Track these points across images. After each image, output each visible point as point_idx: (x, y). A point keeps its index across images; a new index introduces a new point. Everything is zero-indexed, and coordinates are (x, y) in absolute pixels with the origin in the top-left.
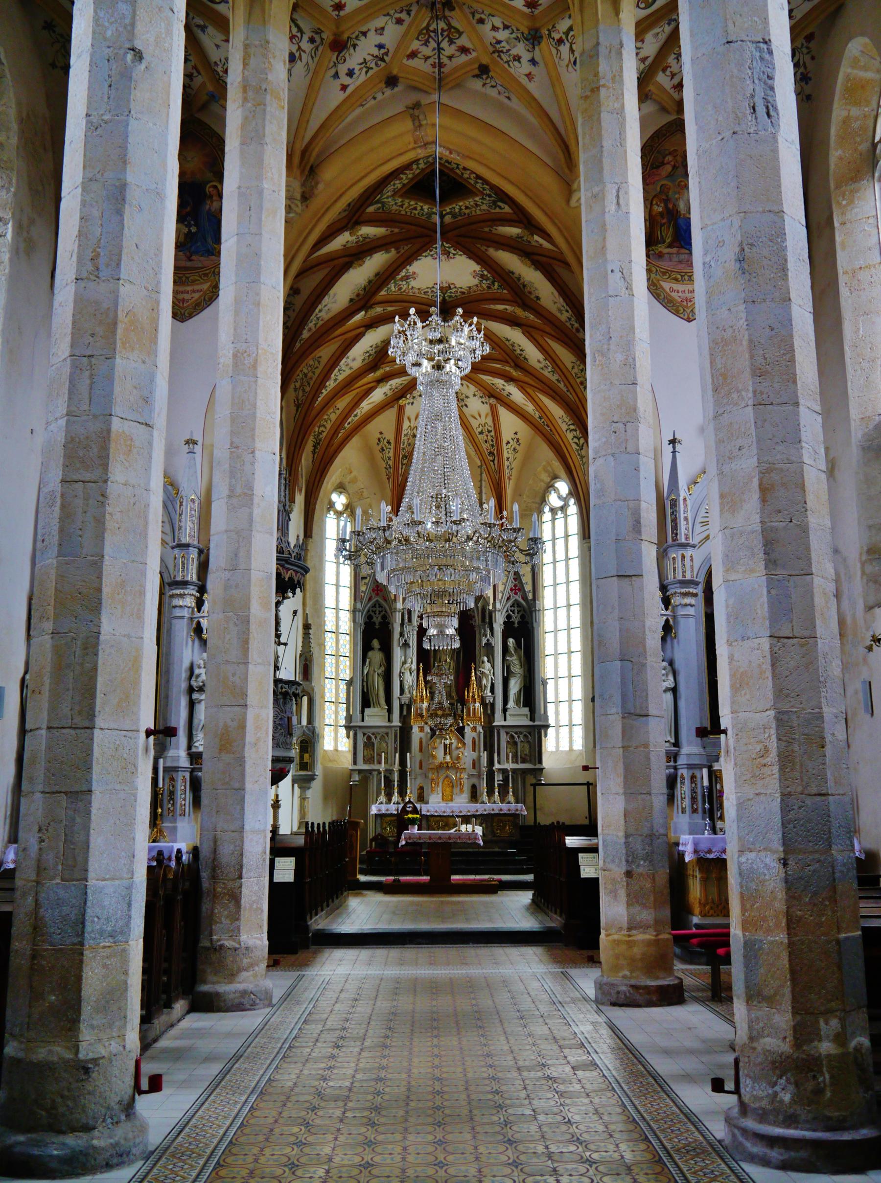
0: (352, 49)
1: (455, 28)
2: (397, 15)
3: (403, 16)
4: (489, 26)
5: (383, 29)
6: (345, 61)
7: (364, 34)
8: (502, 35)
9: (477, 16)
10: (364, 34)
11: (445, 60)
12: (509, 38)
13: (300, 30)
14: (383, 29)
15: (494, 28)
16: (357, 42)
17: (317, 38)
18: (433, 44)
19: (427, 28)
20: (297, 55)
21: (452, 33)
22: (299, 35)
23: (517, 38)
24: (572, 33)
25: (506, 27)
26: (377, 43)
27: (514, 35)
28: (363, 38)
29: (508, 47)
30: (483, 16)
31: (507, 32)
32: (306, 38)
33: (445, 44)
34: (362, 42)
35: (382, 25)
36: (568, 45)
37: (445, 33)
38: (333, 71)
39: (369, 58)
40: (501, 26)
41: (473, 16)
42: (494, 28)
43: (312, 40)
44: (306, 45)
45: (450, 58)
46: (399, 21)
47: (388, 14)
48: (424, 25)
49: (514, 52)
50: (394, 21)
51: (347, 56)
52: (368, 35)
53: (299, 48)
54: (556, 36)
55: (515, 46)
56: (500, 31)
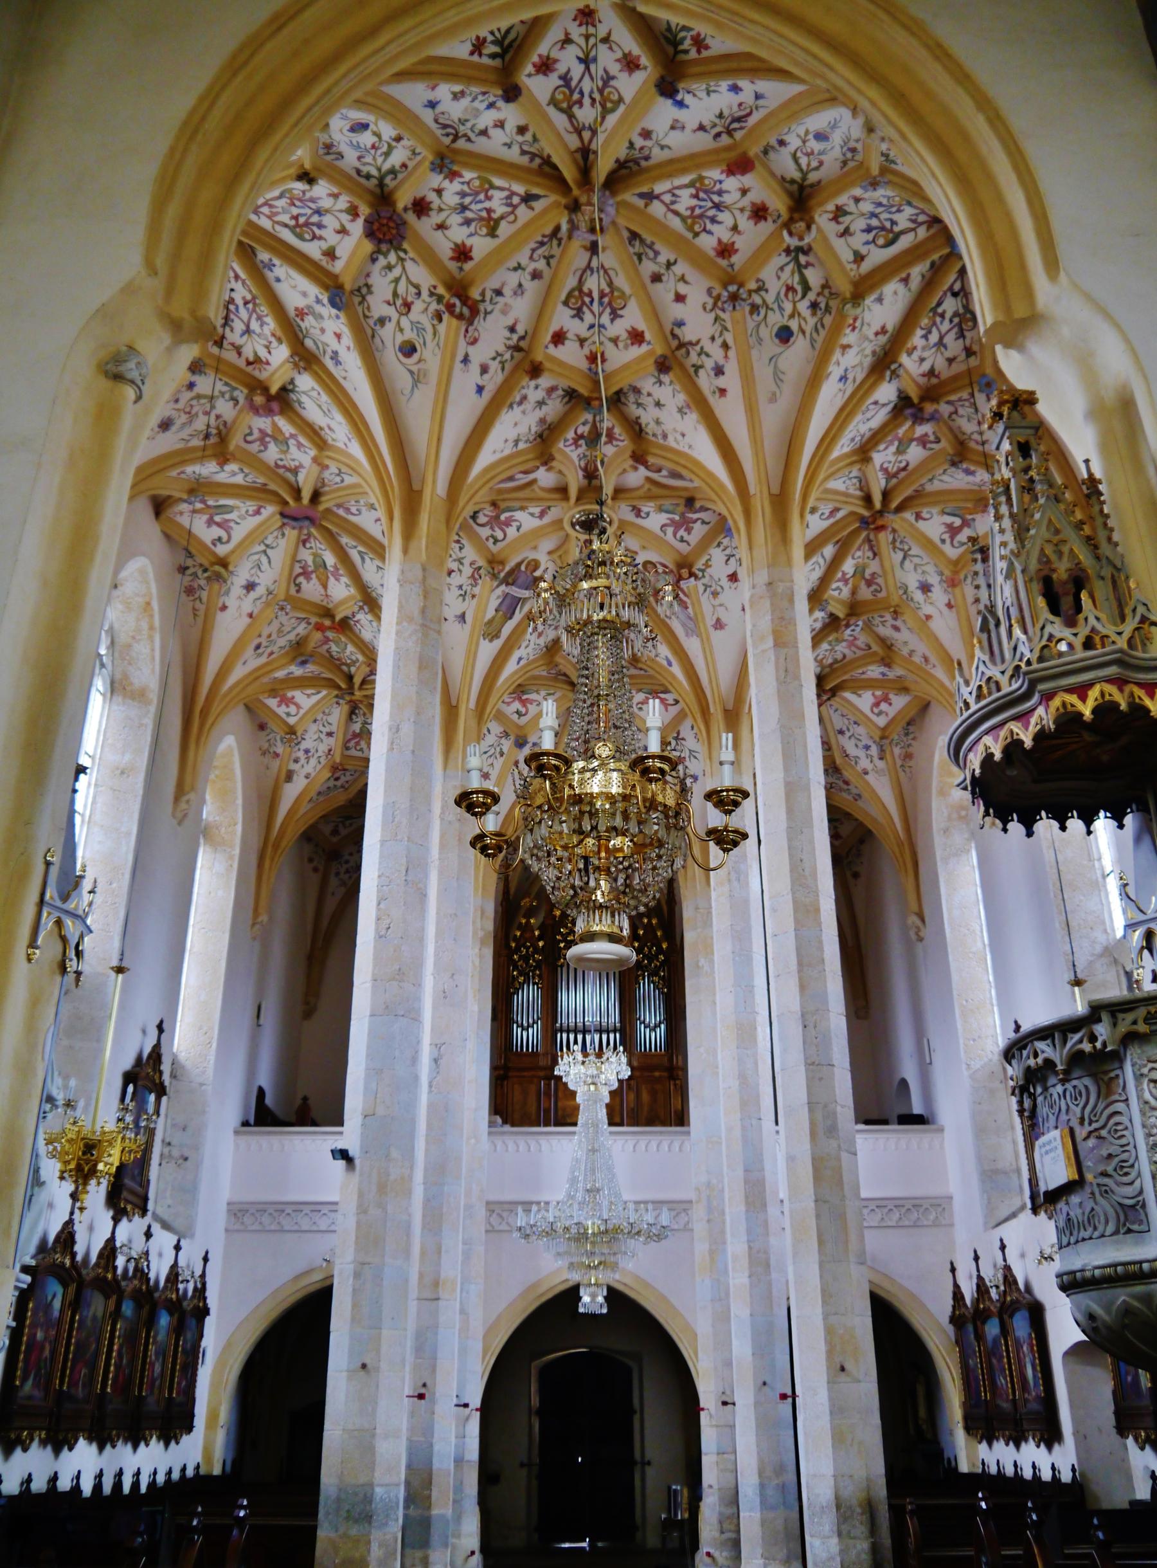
0: (726, 113)
1: (561, 110)
2: (648, 143)
3: (639, 142)
4: (510, 126)
5: (673, 128)
6: (740, 105)
7: (701, 128)
8: (487, 119)
9: (528, 136)
10: (701, 128)
11: (576, 32)
12: (476, 117)
13: (796, 160)
14: (673, 128)
15: (500, 124)
16: (717, 121)
17: (773, 142)
18: (597, 70)
19: (605, 112)
20: (811, 136)
21: (567, 99)
22: (799, 154)
23: (463, 122)
24: (385, 149)
25: (484, 133)
26: (684, 111)
27: (469, 125)
28: (706, 123)
29: (476, 104)
30: (520, 138)
31: (481, 126)
32: (791, 148)
33: (577, 70)
34: (708, 118)
35: (673, 133)
36: (385, 137)
37: (576, 96)
38: (761, 102)
39: (703, 95)
40: (491, 132)
41: (534, 136)
42: (500, 124)
43: (782, 143)
44: (794, 142)
45: (567, 41)
46: (646, 134)
47: (662, 147)
48: (612, 119)
49: (465, 102)
50: (654, 136)
51: (735, 108)
52: (696, 126)
53: (804, 142)
54: (404, 142)
55: (466, 109)
56: (491, 124)
